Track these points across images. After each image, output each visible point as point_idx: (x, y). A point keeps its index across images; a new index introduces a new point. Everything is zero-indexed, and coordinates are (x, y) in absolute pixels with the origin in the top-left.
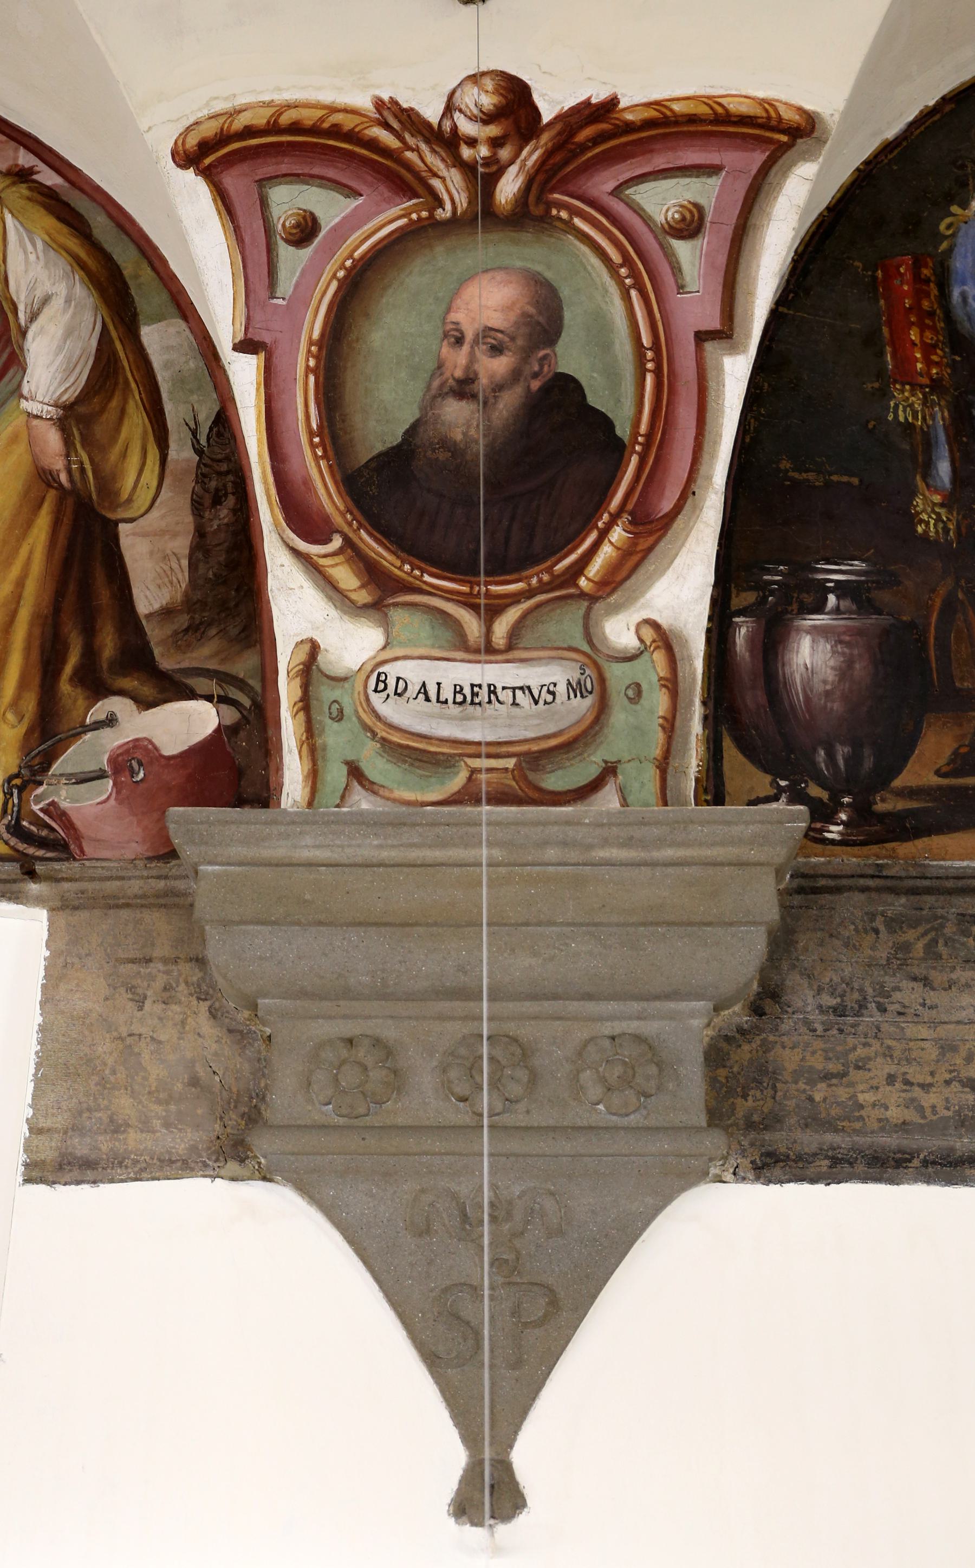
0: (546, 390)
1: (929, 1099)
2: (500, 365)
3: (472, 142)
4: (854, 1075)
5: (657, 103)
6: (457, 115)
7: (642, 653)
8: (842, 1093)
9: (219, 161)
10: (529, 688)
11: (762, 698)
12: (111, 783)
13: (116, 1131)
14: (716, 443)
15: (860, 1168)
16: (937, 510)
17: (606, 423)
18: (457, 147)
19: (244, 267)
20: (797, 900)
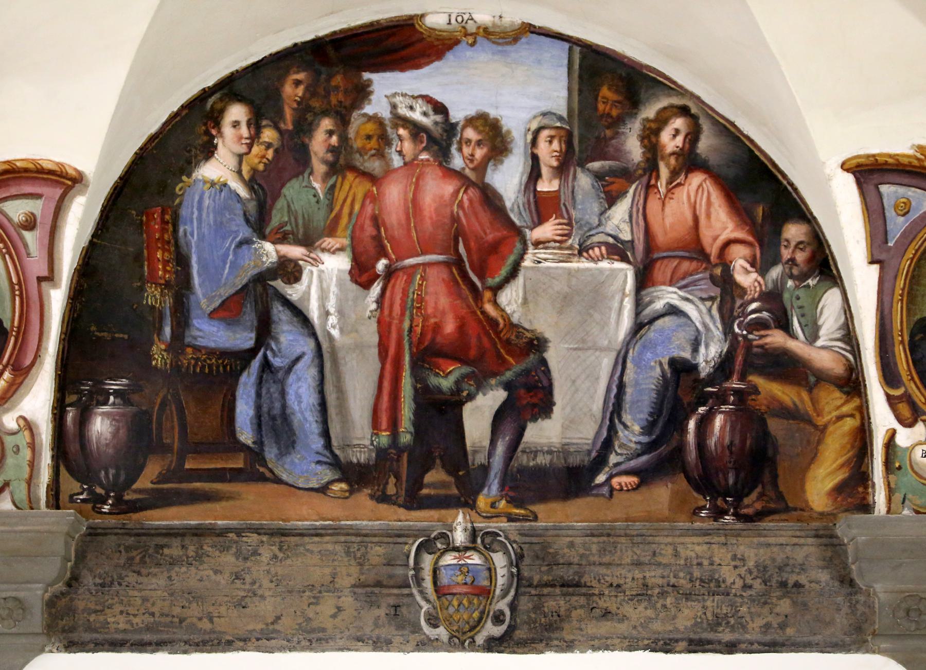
1: (135, 620)
4: (107, 611)
16: (163, 353)
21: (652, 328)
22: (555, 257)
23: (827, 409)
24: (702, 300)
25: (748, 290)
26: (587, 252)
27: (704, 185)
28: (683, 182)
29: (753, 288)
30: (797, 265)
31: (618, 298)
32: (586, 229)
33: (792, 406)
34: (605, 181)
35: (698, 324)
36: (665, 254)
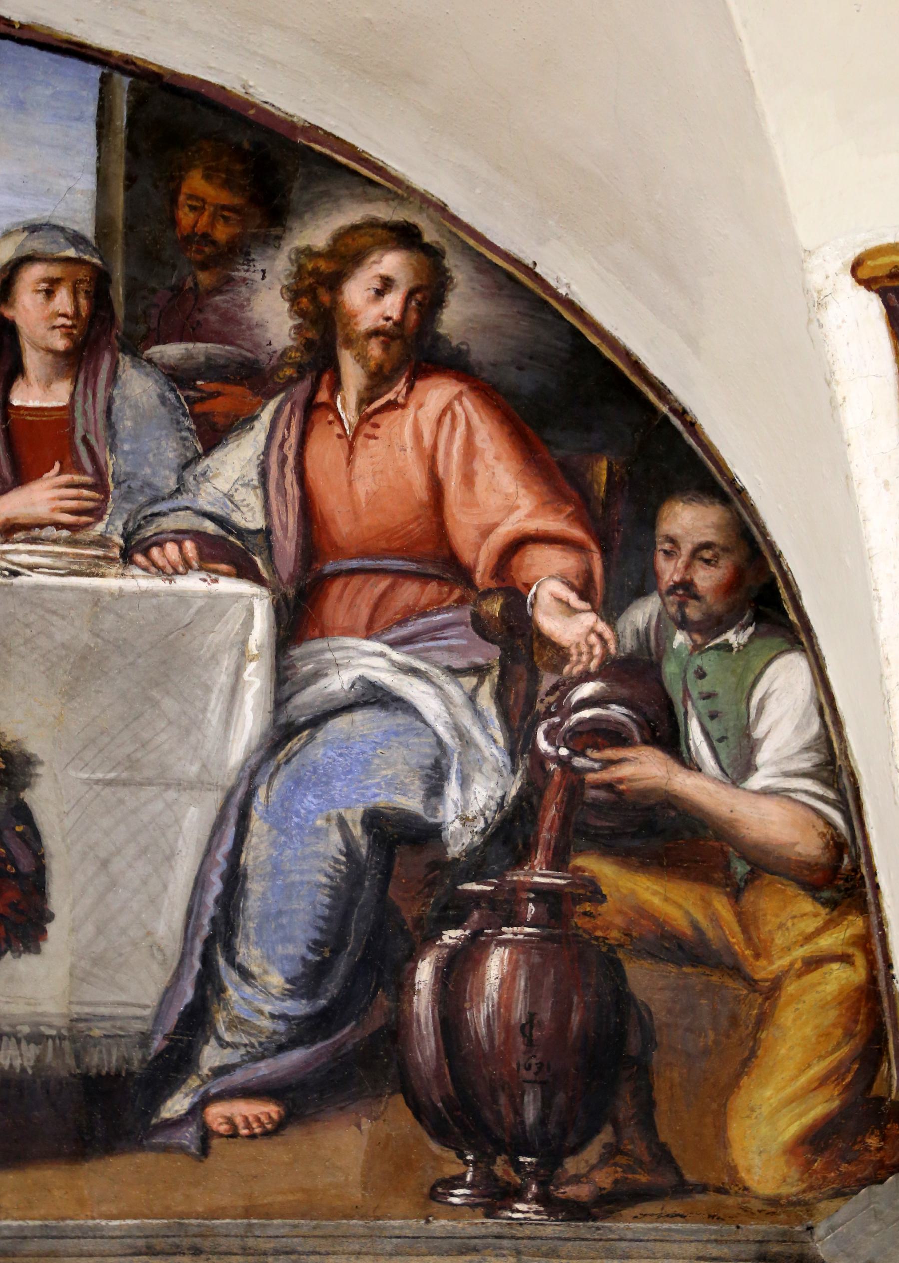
21: (320, 736)
22: (59, 563)
23: (779, 940)
24: (454, 672)
25: (574, 651)
26: (146, 553)
27: (458, 408)
28: (400, 400)
29: (584, 649)
30: (697, 597)
31: (227, 662)
32: (142, 499)
33: (689, 932)
34: (195, 388)
35: (440, 730)
36: (354, 564)
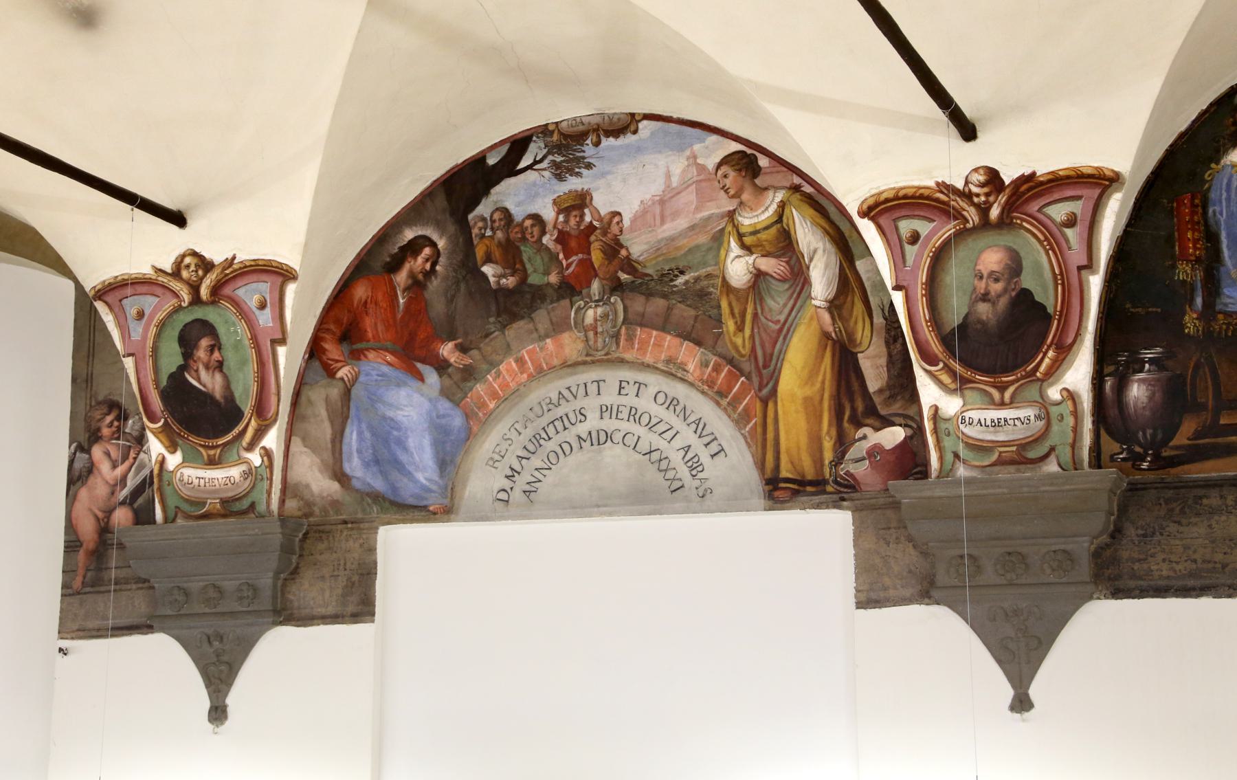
0: (1018, 295)
1: (1178, 567)
2: (998, 287)
3: (978, 195)
4: (1150, 559)
5: (1053, 172)
6: (970, 185)
7: (1063, 402)
8: (1145, 566)
9: (877, 213)
10: (1020, 418)
11: (1117, 412)
12: (868, 462)
13: (885, 590)
14: (1089, 312)
15: (1151, 593)
16: (1194, 321)
17: (1042, 307)
18: (972, 197)
19: (893, 256)
20: (1129, 493)
